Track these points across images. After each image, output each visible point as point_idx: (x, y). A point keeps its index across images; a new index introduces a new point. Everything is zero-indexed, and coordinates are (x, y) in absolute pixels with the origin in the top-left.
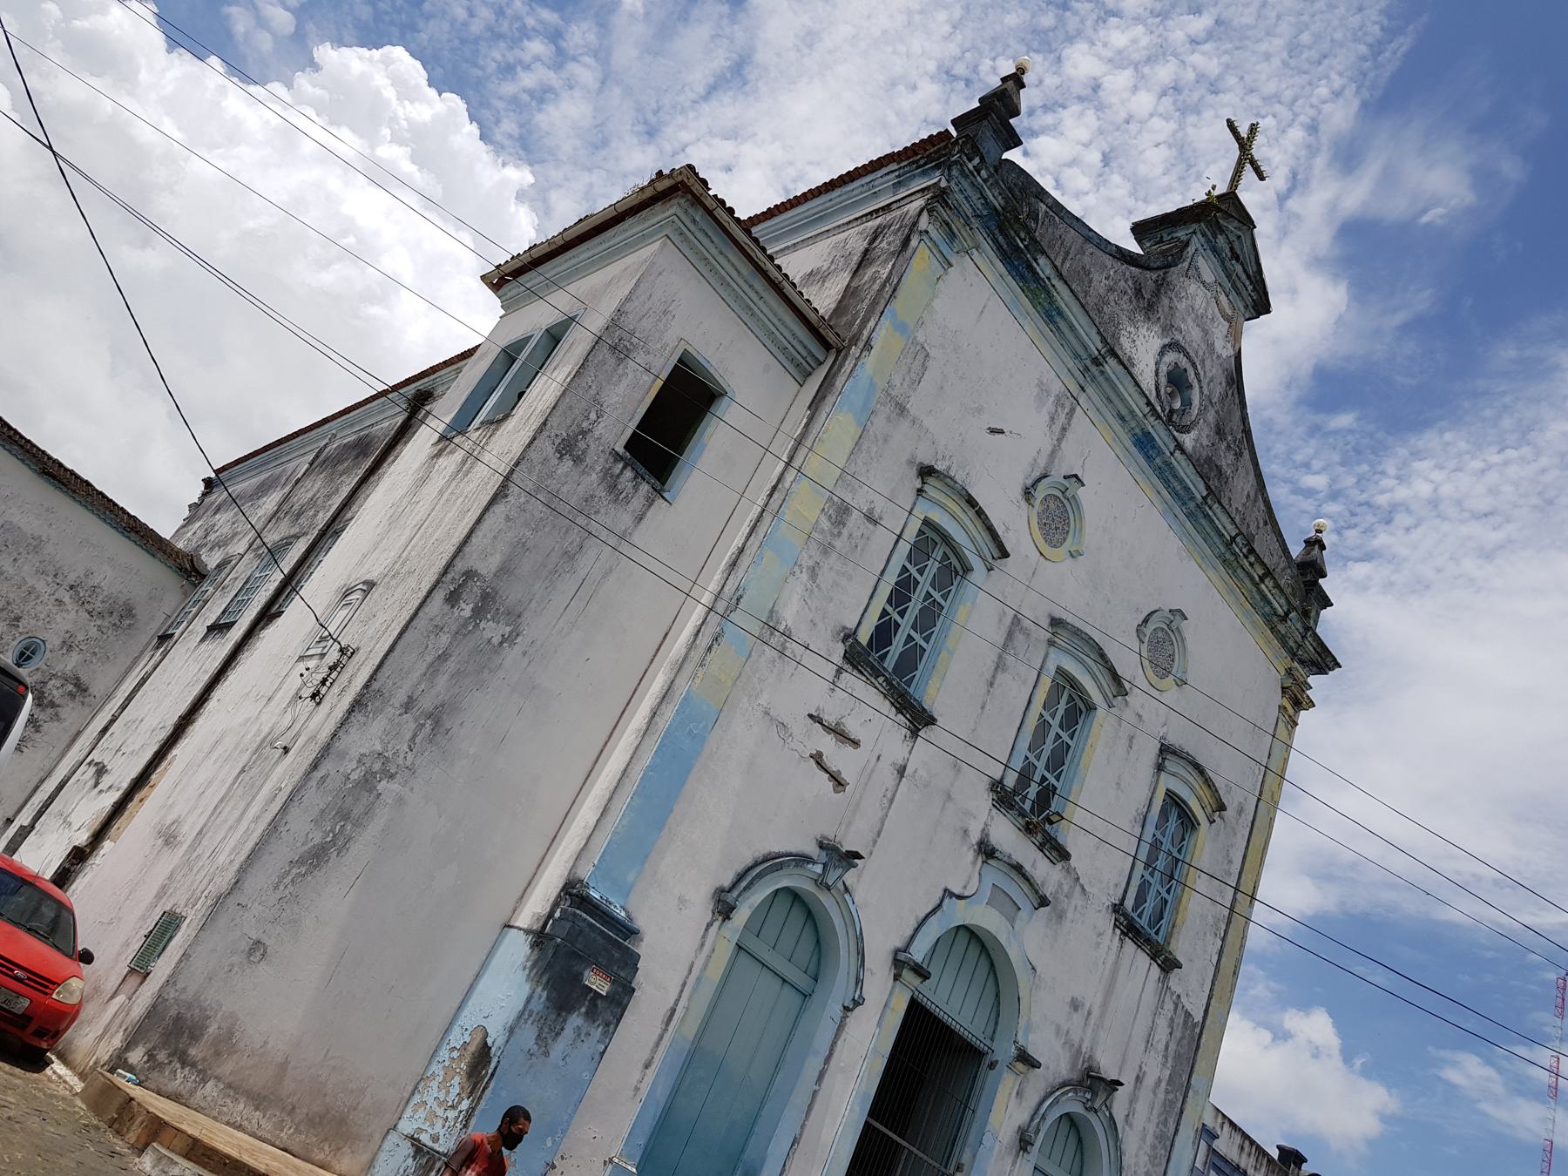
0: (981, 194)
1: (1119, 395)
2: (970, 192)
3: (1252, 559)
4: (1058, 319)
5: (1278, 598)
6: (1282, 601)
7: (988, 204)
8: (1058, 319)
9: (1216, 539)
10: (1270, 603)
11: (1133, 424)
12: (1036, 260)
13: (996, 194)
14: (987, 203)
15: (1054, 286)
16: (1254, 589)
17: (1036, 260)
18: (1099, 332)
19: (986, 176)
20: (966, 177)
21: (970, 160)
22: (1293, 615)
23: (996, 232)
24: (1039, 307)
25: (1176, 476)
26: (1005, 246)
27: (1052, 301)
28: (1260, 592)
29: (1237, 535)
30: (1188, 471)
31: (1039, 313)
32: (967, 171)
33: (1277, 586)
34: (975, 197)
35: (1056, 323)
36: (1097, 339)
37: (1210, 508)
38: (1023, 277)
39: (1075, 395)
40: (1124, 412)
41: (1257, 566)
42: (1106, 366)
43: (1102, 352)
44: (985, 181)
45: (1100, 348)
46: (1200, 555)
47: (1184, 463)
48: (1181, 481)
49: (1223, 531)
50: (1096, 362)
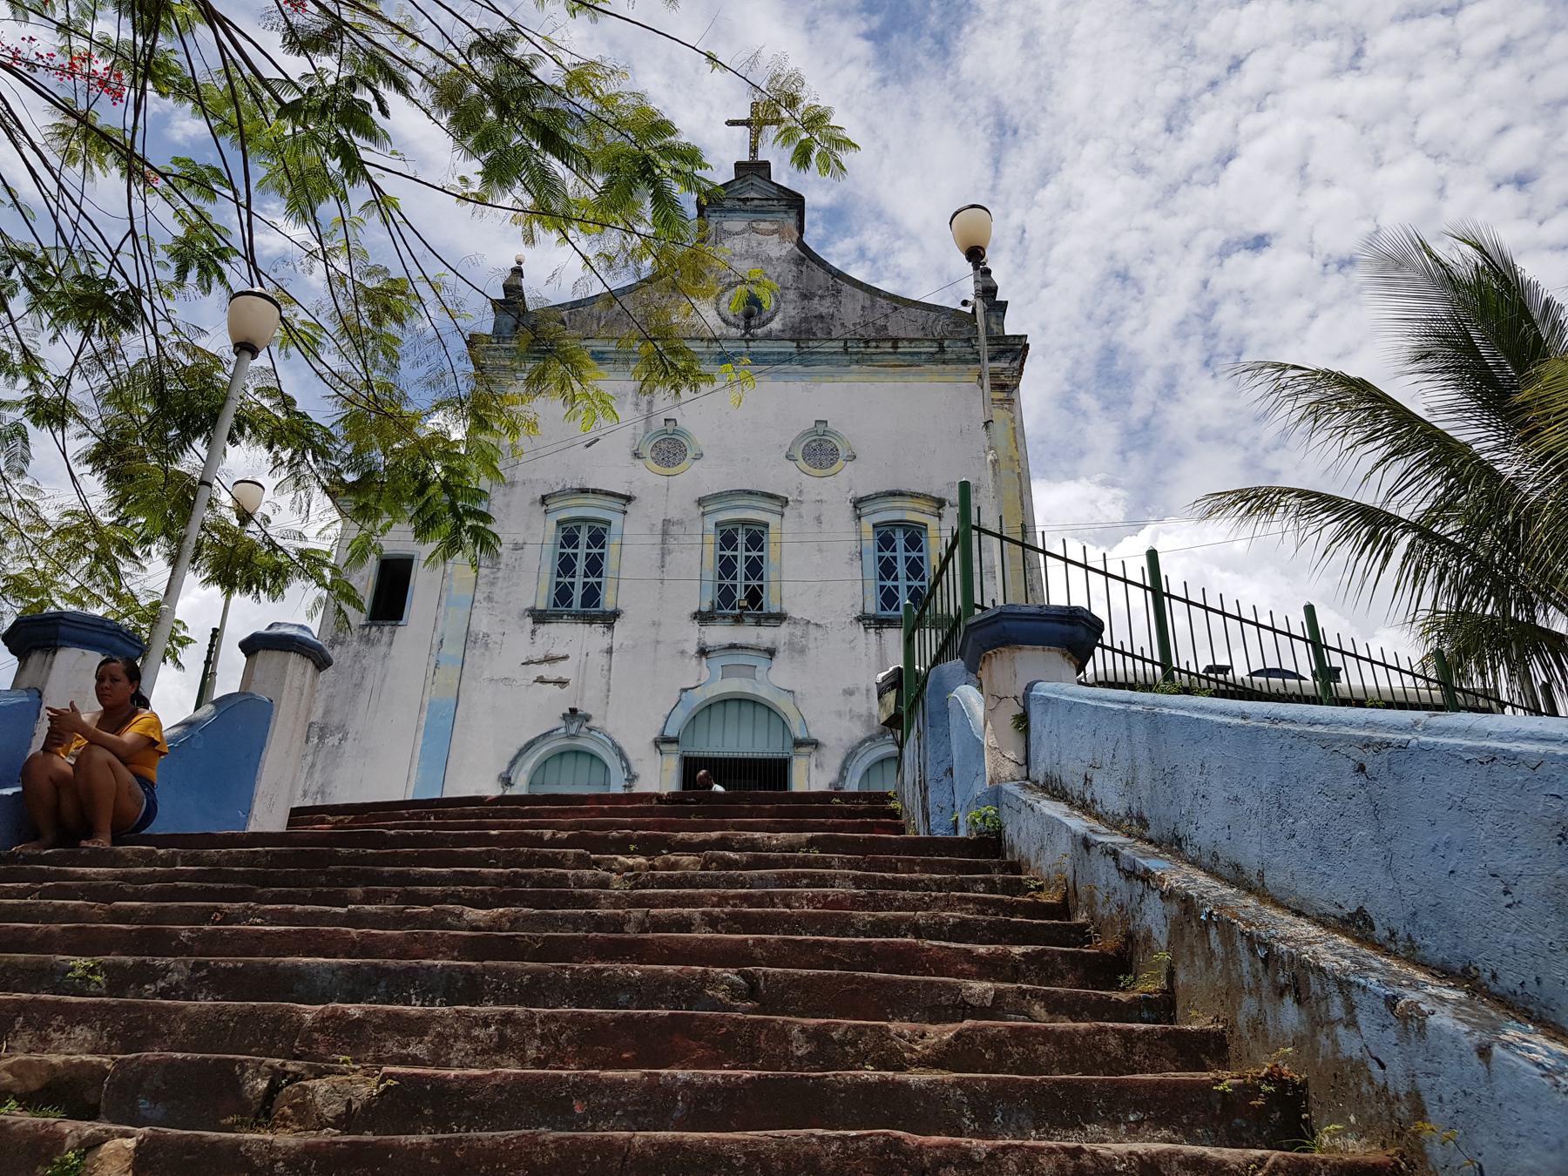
3: (874, 344)
6: (927, 344)
9: (835, 357)
22: (946, 343)
25: (766, 354)
33: (911, 340)
48: (773, 353)
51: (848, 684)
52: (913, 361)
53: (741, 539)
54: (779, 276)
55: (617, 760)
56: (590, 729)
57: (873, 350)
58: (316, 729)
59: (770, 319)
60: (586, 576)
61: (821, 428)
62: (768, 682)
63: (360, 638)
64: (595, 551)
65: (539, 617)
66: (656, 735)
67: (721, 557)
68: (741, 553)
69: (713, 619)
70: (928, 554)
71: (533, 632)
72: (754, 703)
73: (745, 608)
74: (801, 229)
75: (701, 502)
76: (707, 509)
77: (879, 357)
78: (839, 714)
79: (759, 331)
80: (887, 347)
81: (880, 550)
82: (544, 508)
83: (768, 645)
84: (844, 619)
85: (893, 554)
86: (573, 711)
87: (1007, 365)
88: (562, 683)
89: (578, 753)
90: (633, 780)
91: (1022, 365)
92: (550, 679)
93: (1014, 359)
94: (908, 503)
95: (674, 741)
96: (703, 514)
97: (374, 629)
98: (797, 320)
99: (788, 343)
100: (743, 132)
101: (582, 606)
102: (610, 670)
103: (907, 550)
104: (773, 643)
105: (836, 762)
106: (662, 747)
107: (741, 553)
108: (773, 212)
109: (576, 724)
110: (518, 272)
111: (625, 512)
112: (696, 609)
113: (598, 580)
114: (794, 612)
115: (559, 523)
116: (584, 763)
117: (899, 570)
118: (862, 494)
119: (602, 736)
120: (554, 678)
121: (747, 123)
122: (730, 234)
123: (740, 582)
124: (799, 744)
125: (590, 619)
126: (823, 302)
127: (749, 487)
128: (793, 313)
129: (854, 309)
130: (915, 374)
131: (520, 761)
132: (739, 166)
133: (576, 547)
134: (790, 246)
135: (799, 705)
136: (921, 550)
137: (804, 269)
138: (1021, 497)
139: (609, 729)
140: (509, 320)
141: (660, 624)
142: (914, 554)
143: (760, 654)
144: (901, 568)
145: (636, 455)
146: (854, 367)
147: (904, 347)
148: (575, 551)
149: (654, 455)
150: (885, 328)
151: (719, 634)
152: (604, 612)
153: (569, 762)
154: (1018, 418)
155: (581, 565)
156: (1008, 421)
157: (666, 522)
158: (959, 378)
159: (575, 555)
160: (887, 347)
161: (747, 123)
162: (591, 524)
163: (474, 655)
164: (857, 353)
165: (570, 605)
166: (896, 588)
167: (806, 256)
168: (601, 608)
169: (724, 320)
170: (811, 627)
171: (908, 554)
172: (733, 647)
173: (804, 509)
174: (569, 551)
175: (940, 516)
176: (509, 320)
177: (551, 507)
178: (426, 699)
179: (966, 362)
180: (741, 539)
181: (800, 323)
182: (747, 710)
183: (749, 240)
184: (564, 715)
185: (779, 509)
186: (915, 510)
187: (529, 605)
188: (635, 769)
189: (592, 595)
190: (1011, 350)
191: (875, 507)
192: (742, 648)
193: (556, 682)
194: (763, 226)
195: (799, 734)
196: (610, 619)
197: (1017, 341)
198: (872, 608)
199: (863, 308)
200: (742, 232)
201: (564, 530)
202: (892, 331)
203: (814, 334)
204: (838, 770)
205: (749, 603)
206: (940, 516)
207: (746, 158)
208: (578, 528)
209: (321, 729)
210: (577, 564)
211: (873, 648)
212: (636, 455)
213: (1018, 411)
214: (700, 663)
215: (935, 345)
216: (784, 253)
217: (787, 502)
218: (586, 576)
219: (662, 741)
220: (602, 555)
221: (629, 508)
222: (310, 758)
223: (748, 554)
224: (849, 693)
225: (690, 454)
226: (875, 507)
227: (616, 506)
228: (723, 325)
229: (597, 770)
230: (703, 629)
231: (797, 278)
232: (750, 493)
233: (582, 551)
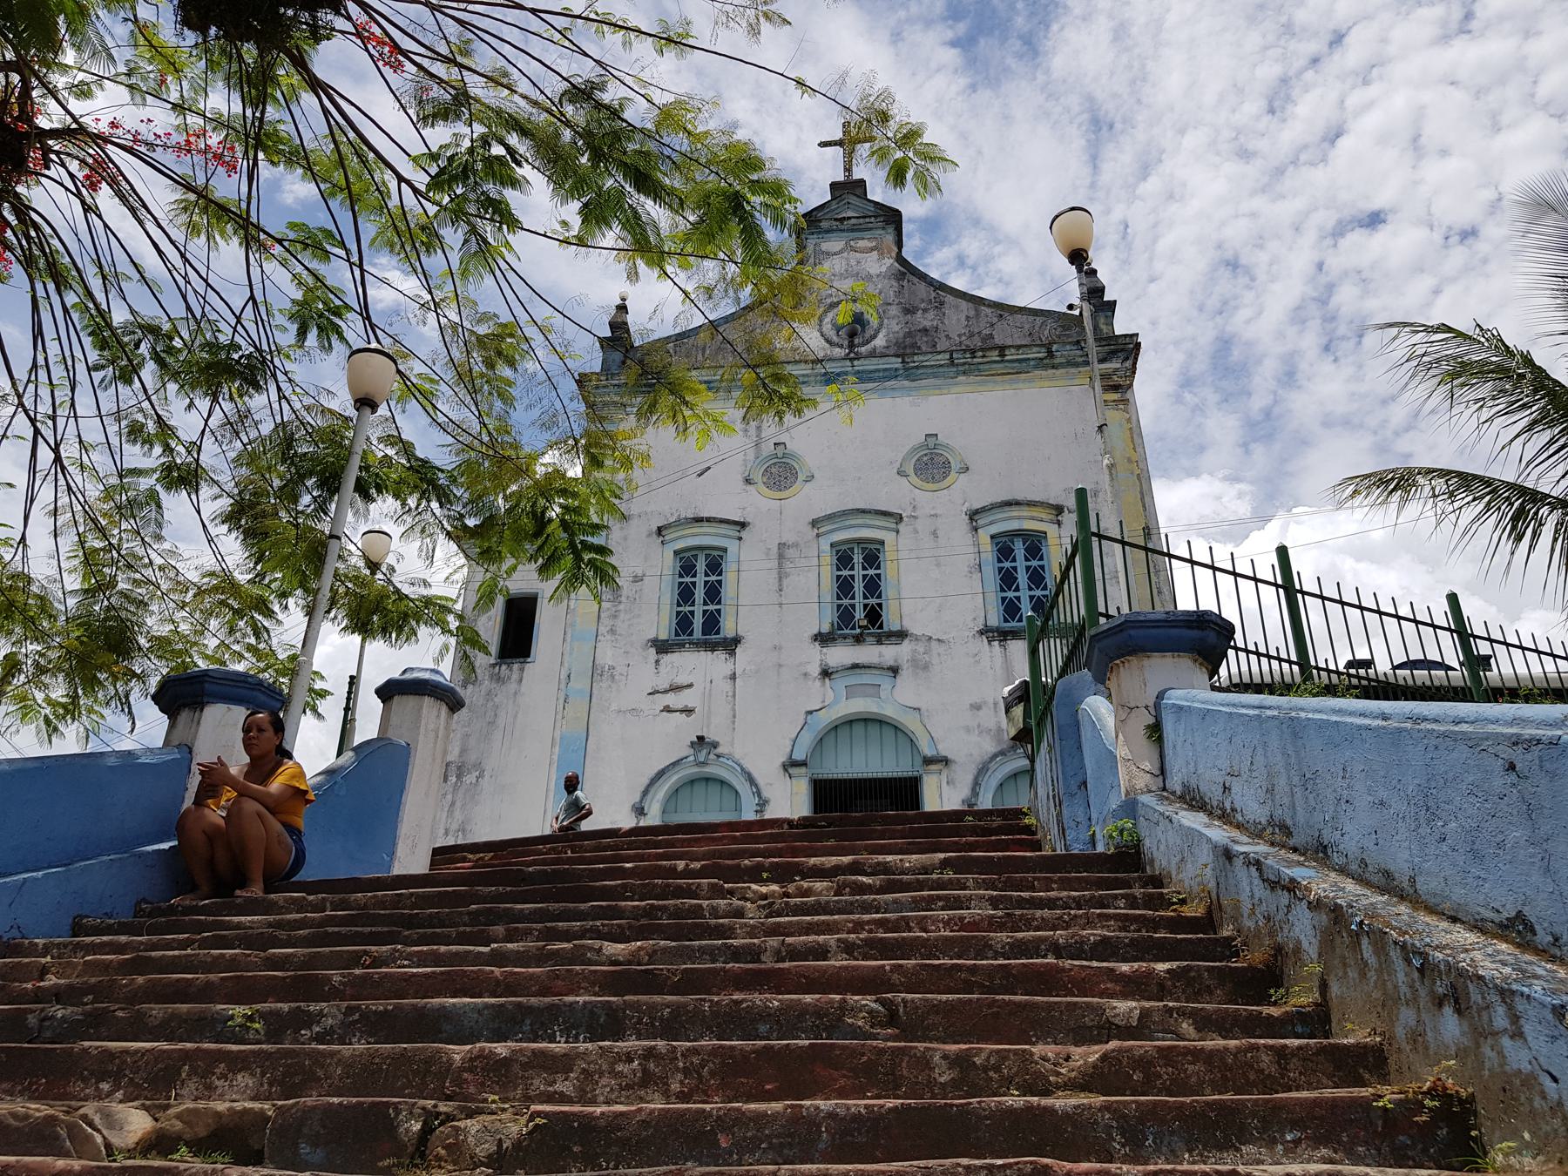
3: (980, 354)
6: (1035, 349)
9: (941, 370)
22: (1055, 347)
25: (871, 372)
29: (951, 355)
33: (1019, 347)
41: (988, 354)
51: (975, 699)
52: (1022, 368)
53: (858, 558)
55: (747, 785)
56: (718, 756)
58: (453, 768)
59: (874, 337)
60: (705, 603)
61: (931, 442)
62: (893, 701)
63: (491, 676)
65: (662, 647)
66: (783, 758)
67: (838, 577)
68: (858, 572)
69: (834, 640)
70: (1049, 561)
71: (657, 662)
72: (880, 722)
73: (866, 627)
75: (814, 523)
76: (821, 530)
77: (987, 367)
78: (968, 730)
80: (994, 356)
81: (999, 561)
83: (891, 663)
84: (967, 633)
85: (1013, 564)
86: (701, 738)
87: (1119, 366)
88: (688, 711)
89: (708, 780)
91: (1135, 364)
92: (676, 707)
93: (1127, 359)
94: (1025, 512)
95: (803, 764)
96: (818, 536)
97: (504, 667)
98: (901, 335)
99: (893, 359)
100: (839, 150)
101: (704, 634)
102: (734, 696)
103: (1027, 559)
104: (896, 661)
105: (969, 779)
106: (792, 771)
107: (858, 572)
108: (871, 229)
109: (704, 752)
110: (622, 308)
111: (740, 539)
112: (816, 631)
113: (718, 607)
115: (676, 553)
116: (714, 789)
117: (1020, 580)
119: (730, 762)
120: (680, 707)
121: (839, 143)
122: (828, 254)
123: (859, 601)
124: (928, 761)
125: (711, 647)
126: (927, 315)
127: (862, 506)
128: (897, 328)
129: (959, 320)
130: (1024, 381)
131: (652, 791)
134: (889, 262)
135: (926, 721)
136: (1041, 559)
137: (905, 283)
138: (1142, 499)
139: (737, 755)
140: (617, 356)
141: (780, 648)
142: (1035, 563)
143: (884, 673)
144: (1022, 578)
145: (748, 481)
146: (961, 378)
150: (991, 336)
151: (841, 655)
152: (725, 639)
153: (700, 789)
154: (1134, 418)
155: (699, 594)
157: (781, 546)
158: (1069, 383)
159: (694, 584)
160: (994, 356)
161: (839, 143)
162: (708, 552)
163: (601, 687)
164: (964, 364)
165: (691, 634)
166: (1018, 598)
167: (907, 271)
168: (722, 635)
169: (828, 341)
170: (934, 643)
171: (1029, 563)
172: (855, 666)
173: (919, 525)
174: (688, 579)
175: (1059, 523)
176: (617, 356)
177: (667, 538)
178: (558, 734)
179: (1077, 365)
180: (858, 558)
181: (905, 337)
182: (874, 730)
185: (894, 526)
186: (1033, 518)
187: (652, 636)
188: (765, 794)
189: (712, 622)
190: (1122, 350)
191: (992, 518)
192: (864, 667)
193: (682, 711)
194: (861, 244)
195: (928, 751)
196: (731, 645)
197: (1128, 340)
198: (995, 620)
199: (968, 318)
202: (998, 340)
203: (919, 348)
204: (970, 786)
205: (869, 622)
206: (1059, 523)
207: (841, 177)
208: (695, 557)
209: (459, 768)
210: (696, 592)
211: (999, 660)
212: (748, 481)
213: (1134, 411)
214: (823, 684)
216: (884, 269)
217: (901, 518)
218: (705, 603)
219: (791, 765)
220: (720, 582)
221: (744, 534)
222: (449, 797)
223: (865, 572)
224: (976, 707)
225: (801, 477)
226: (992, 518)
227: (731, 533)
229: (728, 797)
230: (825, 650)
231: (899, 293)
232: (863, 511)
233: (700, 579)
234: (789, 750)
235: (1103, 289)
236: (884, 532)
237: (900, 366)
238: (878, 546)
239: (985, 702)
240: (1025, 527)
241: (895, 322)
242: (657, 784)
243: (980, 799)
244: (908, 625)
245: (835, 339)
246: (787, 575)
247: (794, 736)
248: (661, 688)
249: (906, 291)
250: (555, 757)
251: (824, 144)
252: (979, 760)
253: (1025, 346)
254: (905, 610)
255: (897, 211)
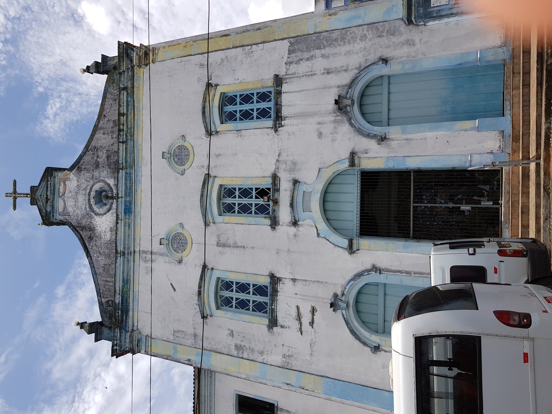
0: (120, 337)
1: (125, 235)
2: (123, 340)
3: (121, 126)
4: (125, 278)
5: (123, 100)
6: (122, 97)
7: (121, 334)
8: (125, 278)
10: (127, 101)
11: (127, 220)
12: (119, 303)
13: (116, 334)
14: (121, 333)
15: (119, 290)
16: (129, 113)
17: (119, 303)
18: (116, 263)
19: (115, 341)
20: (121, 345)
21: (117, 349)
22: (122, 86)
23: (124, 321)
24: (129, 287)
25: (126, 187)
26: (125, 315)
27: (123, 286)
28: (127, 111)
30: (121, 185)
31: (130, 286)
32: (120, 347)
33: (120, 106)
34: (123, 337)
35: (127, 277)
36: (118, 261)
37: (123, 163)
38: (126, 301)
39: (139, 253)
40: (127, 228)
41: (122, 122)
42: (122, 250)
43: (119, 255)
44: (117, 340)
45: (119, 257)
46: (139, 152)
47: (120, 190)
48: (126, 183)
49: (124, 150)
50: (124, 254)
51: (315, 135)
52: (131, 104)
53: (229, 201)
54: (87, 181)
55: (363, 278)
56: (343, 294)
57: (125, 127)
60: (249, 293)
61: (167, 155)
64: (234, 287)
65: (273, 323)
66: (346, 253)
67: (239, 212)
68: (237, 201)
70: (238, 92)
71: (282, 327)
72: (325, 193)
73: (269, 198)
74: (64, 169)
76: (211, 221)
77: (129, 124)
78: (333, 140)
79: (115, 191)
80: (123, 119)
81: (236, 120)
82: (208, 316)
83: (291, 184)
85: (238, 112)
86: (332, 305)
87: (135, 53)
88: (313, 311)
89: (357, 301)
90: (376, 268)
96: (214, 223)
98: (109, 170)
99: (120, 174)
100: (18, 200)
101: (267, 296)
102: (305, 281)
103: (236, 104)
104: (290, 181)
106: (355, 249)
107: (237, 201)
108: (54, 184)
109: (340, 303)
110: (82, 325)
111: (212, 269)
112: (269, 228)
113: (251, 286)
114: (271, 169)
115: (218, 308)
116: (363, 298)
118: (204, 131)
119: (348, 287)
120: (310, 315)
121: (15, 199)
123: (254, 201)
124: (352, 164)
125: (275, 292)
126: (100, 156)
127: (199, 196)
128: (105, 172)
129: (104, 139)
130: (139, 103)
131: (364, 339)
132: (32, 204)
133: (232, 298)
134: (72, 176)
135: (327, 165)
136: (236, 96)
137: (83, 167)
139: (343, 282)
140: (106, 331)
141: (278, 250)
142: (238, 100)
143: (296, 188)
144: (246, 107)
147: (124, 110)
148: (234, 299)
149: (180, 252)
150: (114, 121)
152: (271, 283)
153: (362, 307)
154: (163, 45)
156: (165, 50)
157: (218, 245)
159: (237, 299)
160: (123, 119)
161: (15, 199)
163: (295, 364)
164: (126, 135)
165: (266, 303)
166: (258, 109)
167: (76, 166)
168: (268, 285)
169: (109, 211)
170: (281, 159)
171: (238, 103)
172: (292, 205)
174: (234, 302)
175: (217, 85)
176: (106, 331)
177: (208, 313)
178: (322, 396)
180: (229, 201)
181: (110, 168)
182: (330, 197)
183: (68, 198)
184: (334, 310)
187: (266, 328)
188: (369, 266)
189: (260, 290)
190: (127, 50)
194: (61, 190)
195: (346, 164)
196: (275, 280)
197: (121, 47)
198: (269, 123)
199: (104, 134)
200: (64, 201)
201: (222, 305)
204: (369, 140)
206: (217, 85)
207: (28, 199)
212: (180, 262)
213: (160, 45)
214: (302, 225)
215: (122, 92)
216: (75, 178)
218: (249, 293)
219: (351, 249)
221: (210, 266)
223: (237, 197)
224: (320, 135)
225: (180, 230)
228: (111, 211)
230: (281, 223)
231: (88, 170)
233: (234, 295)
234: (341, 249)
235: (96, 63)
236: (215, 184)
237: (124, 172)
238: (223, 189)
239: (318, 130)
240: (217, 105)
241: (102, 173)
242: (360, 335)
243: (378, 133)
244: (269, 173)
245: (108, 207)
246: (235, 243)
247: (333, 246)
248: (299, 326)
249: (87, 167)
250: (338, 399)
251: (15, 208)
252: (353, 134)
253: (119, 101)
254: (260, 174)
255: (46, 169)
